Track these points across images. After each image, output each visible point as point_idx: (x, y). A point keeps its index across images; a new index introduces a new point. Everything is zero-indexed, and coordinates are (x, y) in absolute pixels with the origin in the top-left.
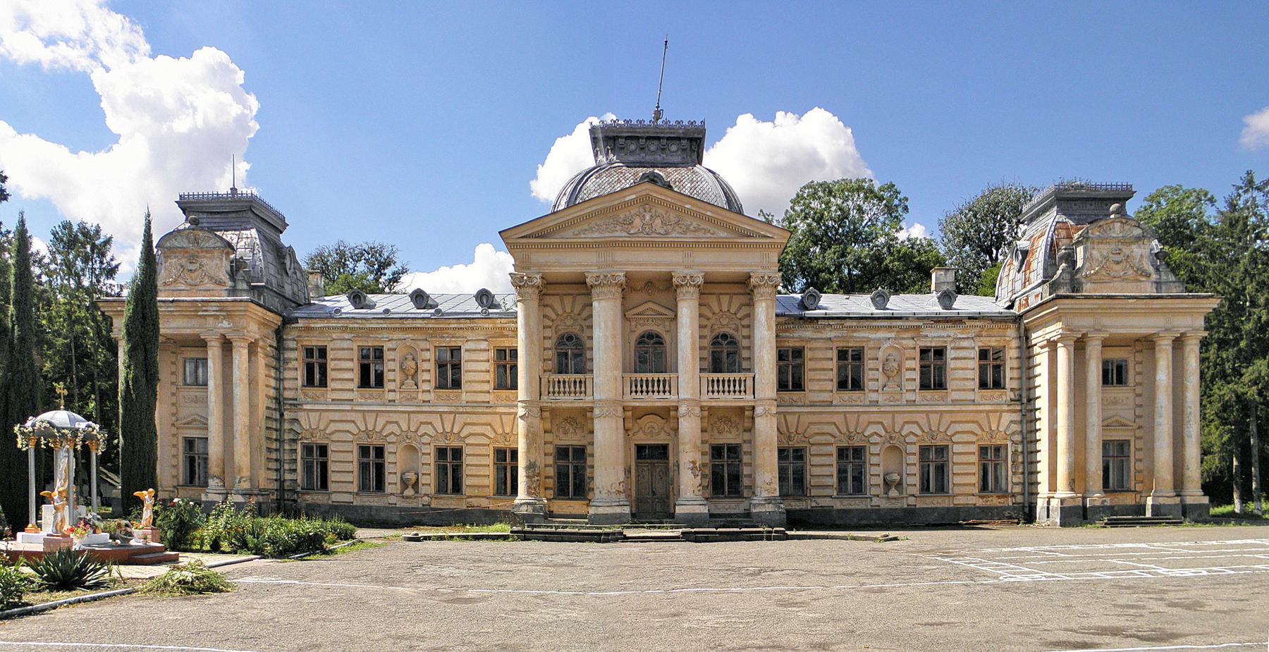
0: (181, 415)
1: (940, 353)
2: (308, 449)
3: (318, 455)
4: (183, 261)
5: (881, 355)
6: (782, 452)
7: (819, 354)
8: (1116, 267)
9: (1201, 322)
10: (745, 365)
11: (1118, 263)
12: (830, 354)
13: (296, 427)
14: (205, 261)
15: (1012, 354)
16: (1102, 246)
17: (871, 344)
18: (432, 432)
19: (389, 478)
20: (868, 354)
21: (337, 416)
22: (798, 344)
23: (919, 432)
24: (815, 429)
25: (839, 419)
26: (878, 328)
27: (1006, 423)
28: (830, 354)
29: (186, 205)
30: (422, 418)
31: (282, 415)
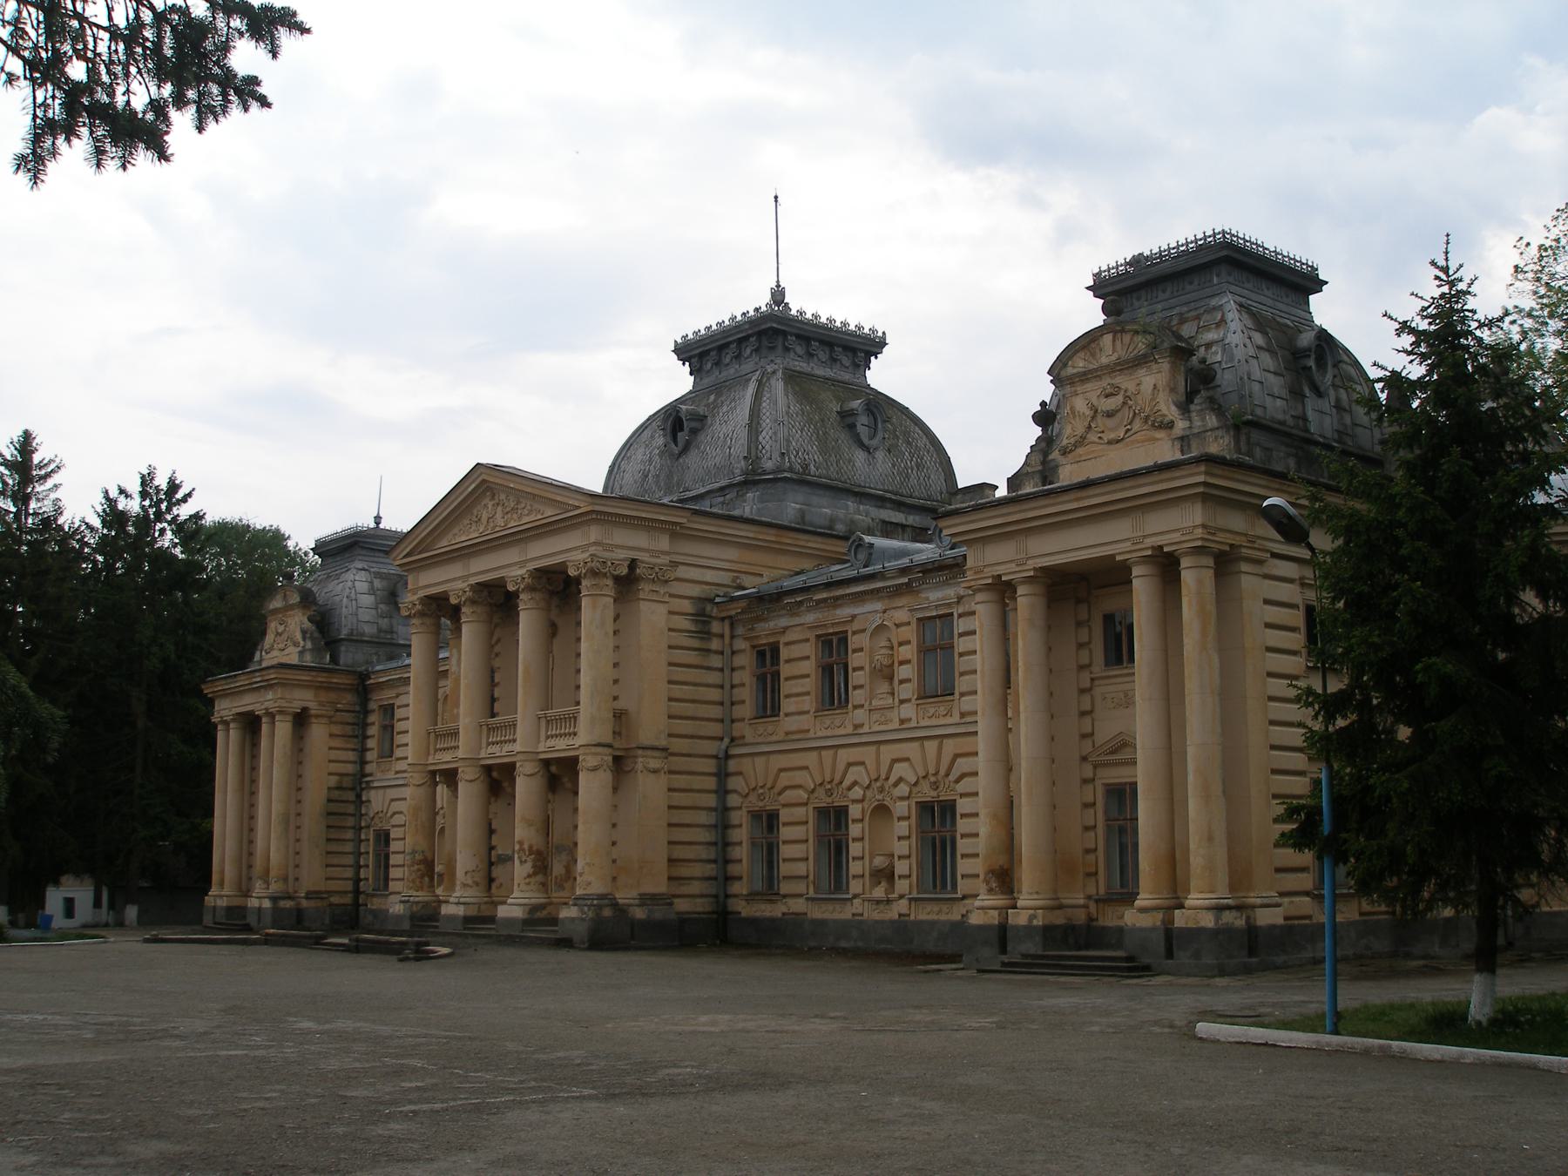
7: (797, 651)
8: (1110, 422)
16: (1089, 386)
17: (856, 626)
22: (771, 640)
24: (785, 779)
26: (860, 598)
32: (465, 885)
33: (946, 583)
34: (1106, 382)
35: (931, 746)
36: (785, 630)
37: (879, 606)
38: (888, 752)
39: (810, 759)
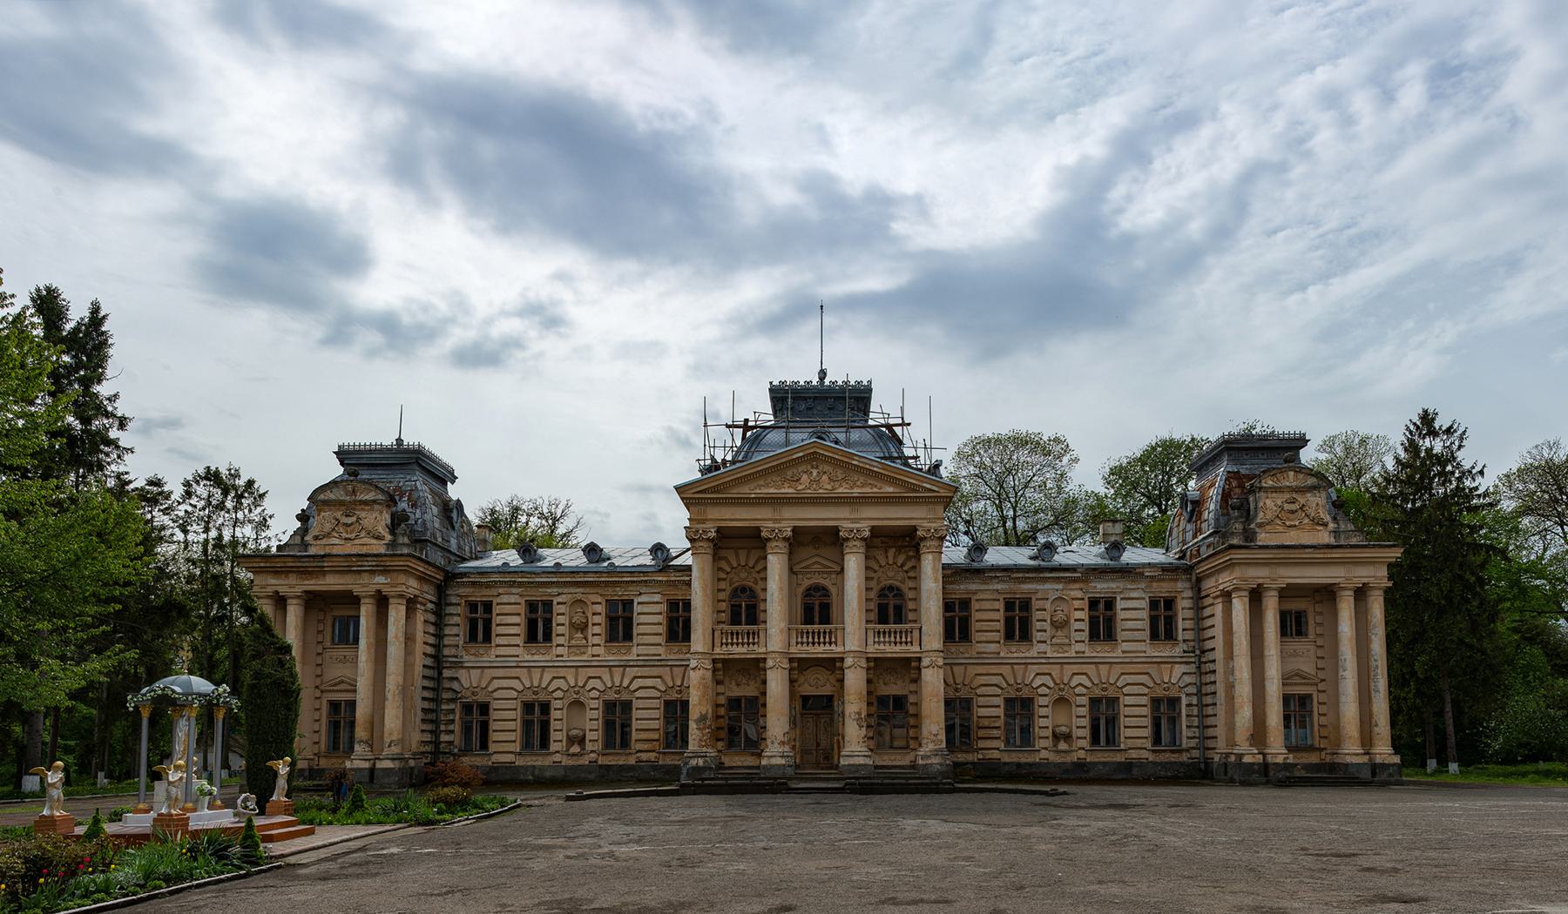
0: (327, 677)
1: (1110, 604)
2: (467, 708)
3: (478, 714)
4: (338, 514)
5: (1048, 605)
6: (948, 703)
9: (1384, 572)
10: (911, 616)
11: (1293, 512)
12: (996, 605)
13: (455, 686)
14: (363, 515)
15: (1183, 605)
18: (600, 686)
19: (554, 736)
20: (1036, 604)
21: (500, 673)
23: (1089, 684)
25: (1006, 670)
27: (1178, 676)
28: (996, 605)
29: (343, 455)
30: (591, 672)
31: (440, 673)
32: (783, 743)
33: (1113, 580)
34: (1287, 496)
35: (1104, 669)
36: (975, 593)
37: (1060, 586)
38: (1069, 670)
39: (1006, 670)
